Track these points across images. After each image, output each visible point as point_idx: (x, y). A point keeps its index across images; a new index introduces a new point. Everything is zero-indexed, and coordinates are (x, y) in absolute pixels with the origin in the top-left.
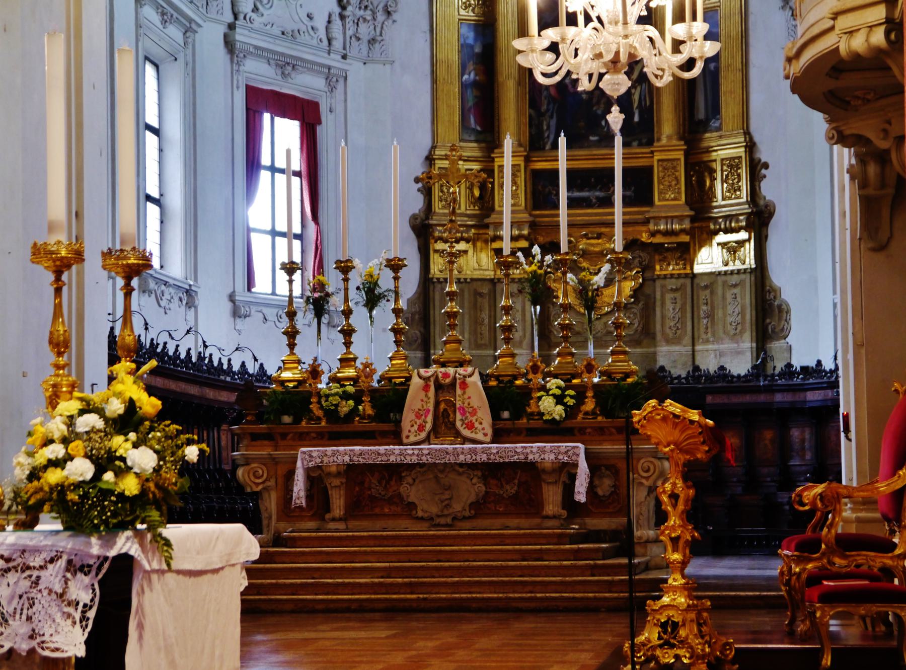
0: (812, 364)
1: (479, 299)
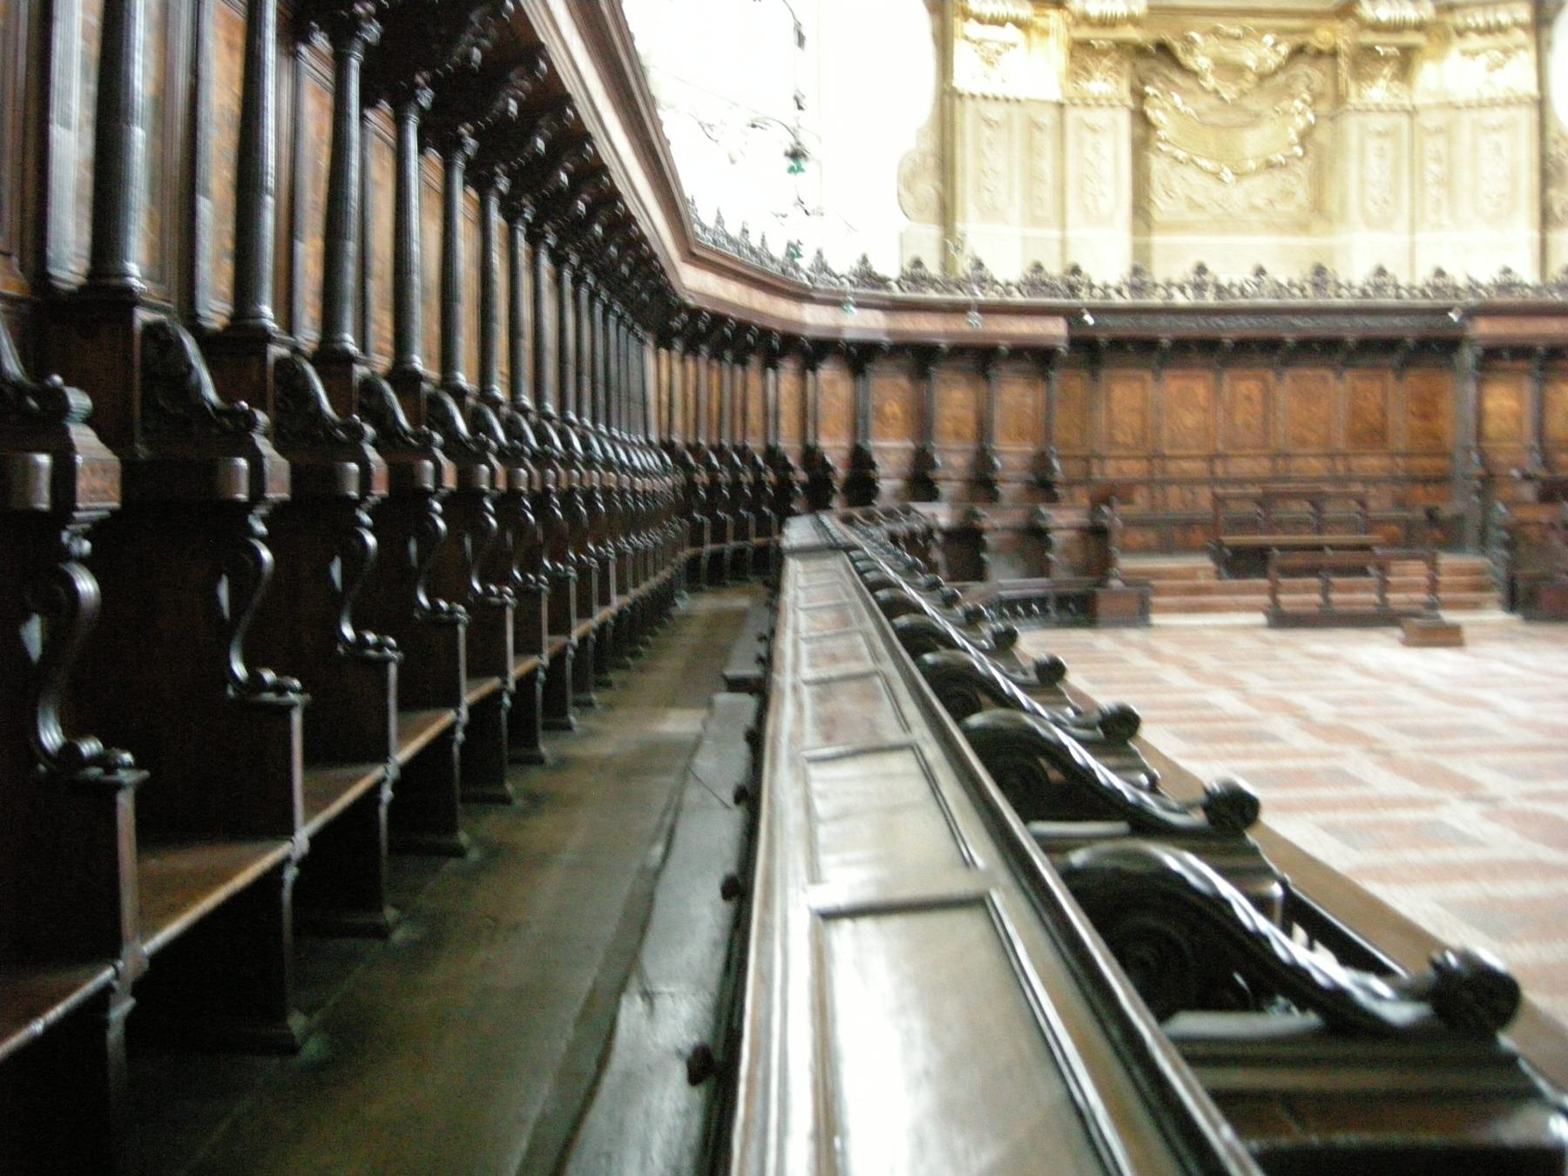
1: (1037, 134)
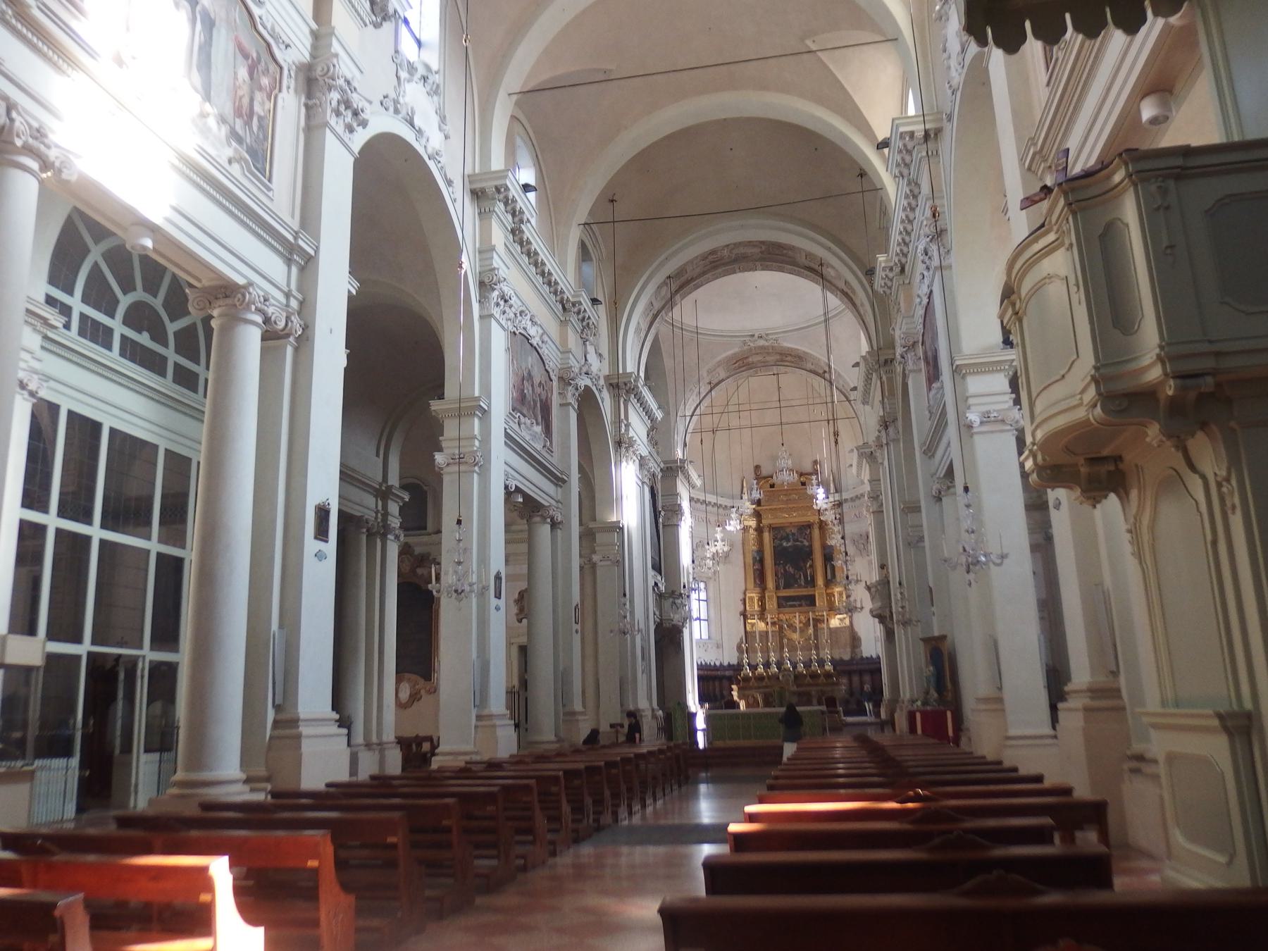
0: (869, 656)
